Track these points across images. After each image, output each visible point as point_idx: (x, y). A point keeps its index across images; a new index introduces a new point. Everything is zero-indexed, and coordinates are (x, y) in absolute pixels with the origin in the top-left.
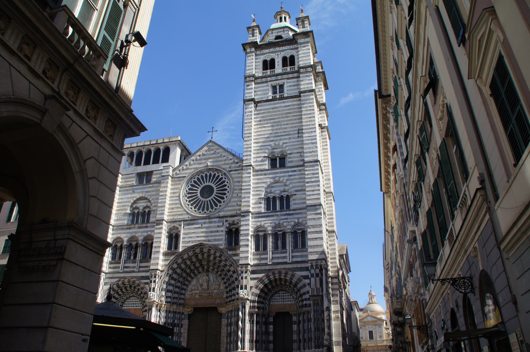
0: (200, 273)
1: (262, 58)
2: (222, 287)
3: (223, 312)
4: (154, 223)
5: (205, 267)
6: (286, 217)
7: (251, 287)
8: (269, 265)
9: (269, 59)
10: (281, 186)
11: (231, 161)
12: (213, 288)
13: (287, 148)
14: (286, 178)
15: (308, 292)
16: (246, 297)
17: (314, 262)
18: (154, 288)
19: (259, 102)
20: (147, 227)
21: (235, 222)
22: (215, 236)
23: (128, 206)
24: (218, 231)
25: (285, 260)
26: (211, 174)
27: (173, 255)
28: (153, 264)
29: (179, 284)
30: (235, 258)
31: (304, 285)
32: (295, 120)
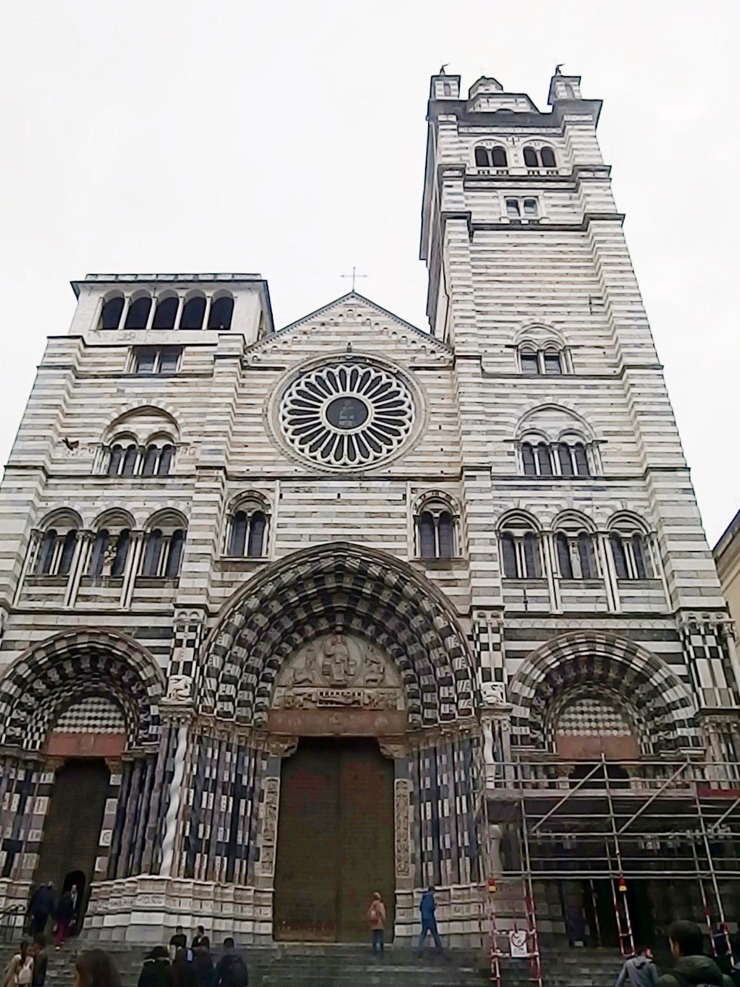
0: (319, 634)
1: (473, 142)
2: (391, 679)
3: (395, 755)
4: (188, 477)
5: (340, 620)
6: (588, 494)
7: (510, 677)
8: (557, 616)
9: (490, 146)
10: (561, 419)
11: (414, 347)
12: (360, 681)
13: (566, 334)
14: (575, 401)
15: (684, 703)
16: (505, 704)
17: (698, 615)
19: (480, 227)
20: (163, 486)
21: (441, 495)
22: (381, 526)
23: (99, 425)
24: (389, 515)
25: (602, 608)
26: (355, 373)
28: (186, 592)
29: (258, 663)
30: (447, 591)
31: (670, 682)
32: (577, 275)
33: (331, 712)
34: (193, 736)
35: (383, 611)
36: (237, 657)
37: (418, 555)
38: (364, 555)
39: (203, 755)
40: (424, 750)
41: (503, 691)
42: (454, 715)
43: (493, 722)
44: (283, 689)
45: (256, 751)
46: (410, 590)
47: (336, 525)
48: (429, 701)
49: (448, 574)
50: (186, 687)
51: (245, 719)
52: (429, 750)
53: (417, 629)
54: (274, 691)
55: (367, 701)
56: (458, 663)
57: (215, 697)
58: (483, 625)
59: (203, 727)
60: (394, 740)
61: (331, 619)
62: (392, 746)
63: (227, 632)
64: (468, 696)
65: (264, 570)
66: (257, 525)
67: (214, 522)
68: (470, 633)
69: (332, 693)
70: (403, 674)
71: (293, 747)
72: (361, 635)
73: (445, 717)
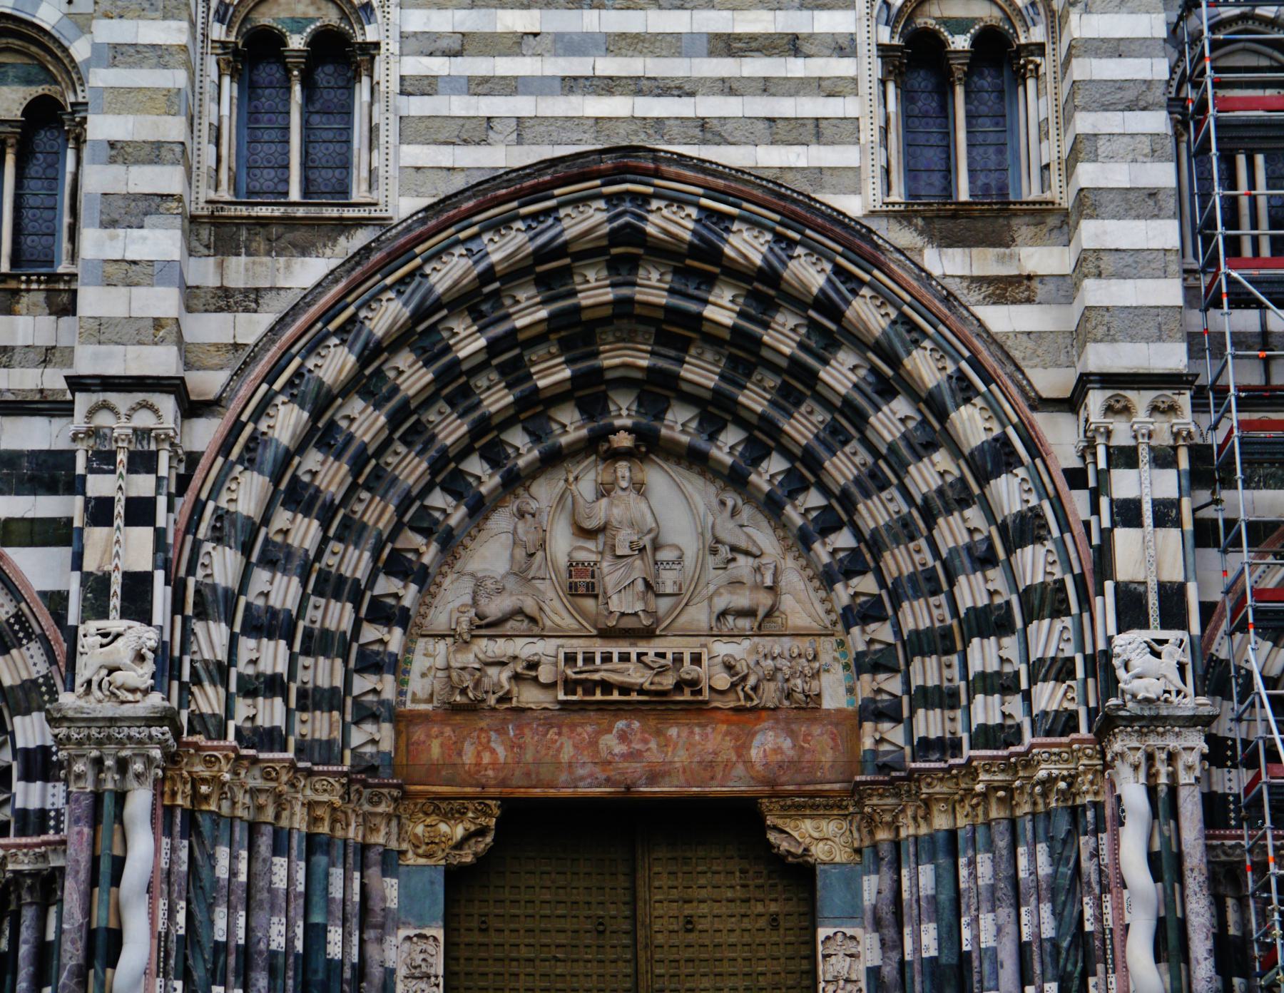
0: (553, 459)
2: (802, 604)
3: (819, 852)
5: (624, 411)
7: (1207, 609)
12: (698, 615)
18: (137, 587)
22: (767, 86)
24: (793, 45)
27: (304, 252)
28: (102, 331)
29: (354, 562)
33: (605, 720)
34: (169, 811)
35: (772, 381)
36: (289, 546)
37: (898, 195)
38: (713, 192)
39: (205, 873)
40: (916, 837)
41: (1187, 659)
42: (1019, 727)
43: (1150, 758)
44: (442, 647)
45: (364, 848)
46: (868, 314)
47: (609, 86)
48: (932, 681)
49: (1001, 259)
50: (140, 658)
51: (328, 751)
52: (931, 837)
53: (892, 447)
54: (408, 650)
55: (722, 680)
56: (1034, 564)
57: (226, 685)
58: (1122, 435)
59: (196, 781)
60: (813, 803)
61: (593, 406)
62: (808, 826)
63: (249, 461)
64: (1063, 670)
65: (366, 250)
66: (324, 75)
67: (177, 78)
68: (1077, 464)
69: (607, 658)
70: (842, 594)
71: (482, 832)
72: (695, 459)
73: (986, 736)
